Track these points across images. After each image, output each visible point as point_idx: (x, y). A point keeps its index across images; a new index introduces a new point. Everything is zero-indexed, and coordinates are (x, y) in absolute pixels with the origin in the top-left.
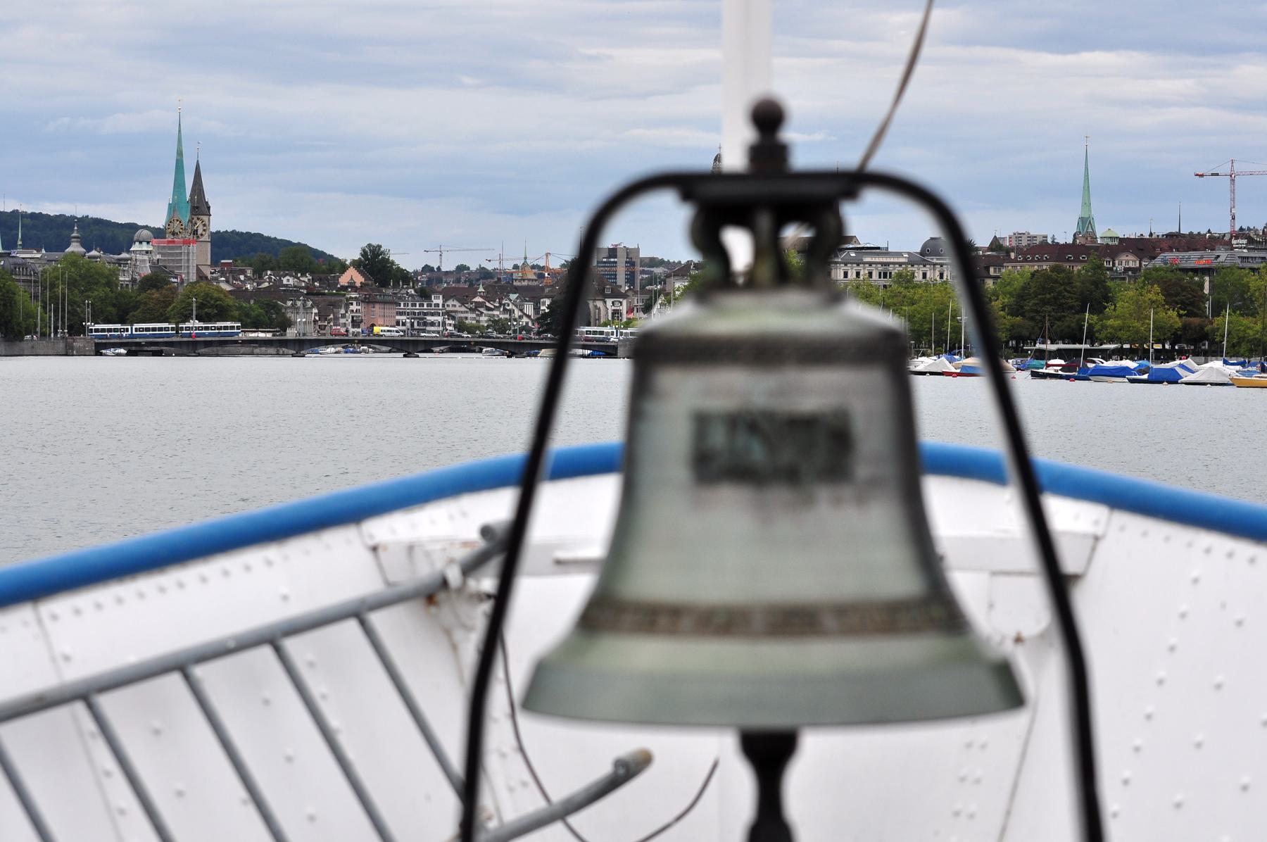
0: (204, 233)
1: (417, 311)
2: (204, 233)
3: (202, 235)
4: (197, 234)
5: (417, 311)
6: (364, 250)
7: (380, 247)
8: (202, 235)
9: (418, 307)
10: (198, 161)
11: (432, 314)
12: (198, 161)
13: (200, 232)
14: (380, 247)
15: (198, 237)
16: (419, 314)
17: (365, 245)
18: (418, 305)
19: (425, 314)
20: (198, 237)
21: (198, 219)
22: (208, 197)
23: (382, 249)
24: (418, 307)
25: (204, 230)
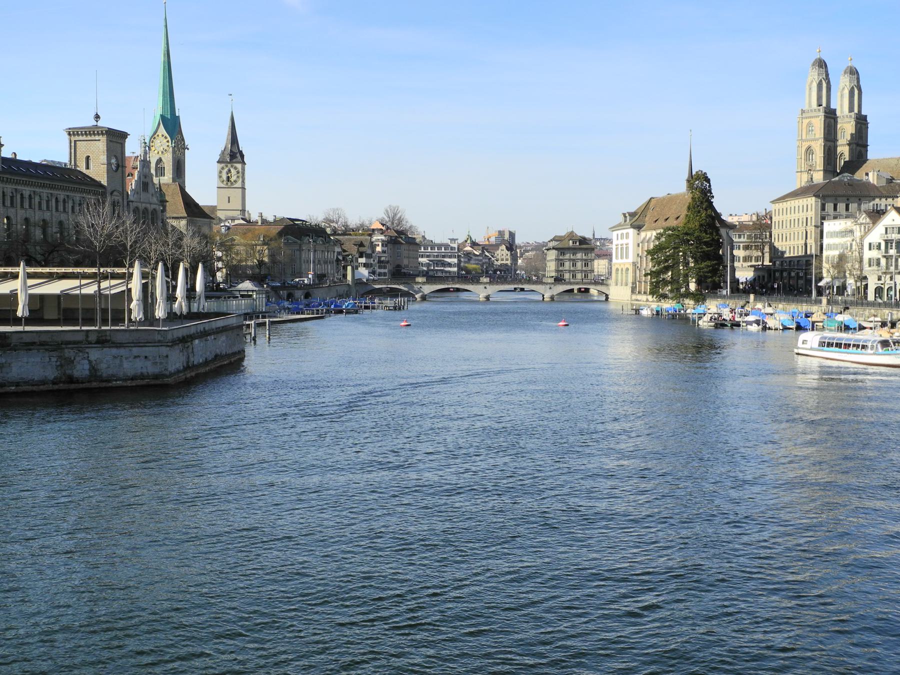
3: (235, 181)
6: (387, 211)
11: (450, 257)
13: (233, 179)
16: (437, 256)
19: (444, 257)
20: (232, 184)
21: (232, 166)
22: (243, 146)
24: (436, 250)
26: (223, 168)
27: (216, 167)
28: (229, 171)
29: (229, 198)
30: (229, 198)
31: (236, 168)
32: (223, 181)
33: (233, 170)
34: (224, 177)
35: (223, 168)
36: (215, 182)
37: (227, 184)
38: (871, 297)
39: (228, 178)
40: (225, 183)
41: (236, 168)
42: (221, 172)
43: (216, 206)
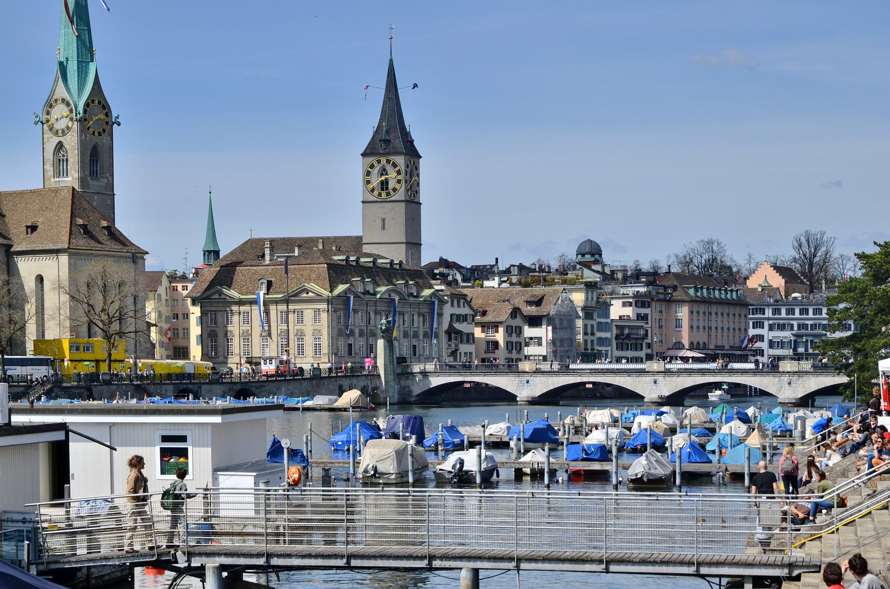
0: (398, 186)
1: (809, 323)
2: (398, 186)
3: (395, 190)
4: (387, 189)
5: (809, 323)
7: (822, 234)
8: (395, 190)
9: (811, 315)
10: (391, 60)
12: (391, 60)
13: (391, 186)
14: (822, 234)
15: (388, 194)
16: (814, 327)
17: (800, 231)
18: (811, 311)
23: (825, 238)
24: (811, 315)
25: (399, 181)
26: (372, 166)
27: (358, 165)
28: (383, 172)
29: (384, 220)
30: (384, 220)
31: (395, 165)
32: (373, 190)
33: (389, 168)
34: (376, 180)
35: (372, 166)
36: (358, 192)
37: (380, 195)
38: (268, 361)
39: (384, 185)
40: (376, 193)
41: (395, 165)
42: (368, 174)
43: (360, 238)
